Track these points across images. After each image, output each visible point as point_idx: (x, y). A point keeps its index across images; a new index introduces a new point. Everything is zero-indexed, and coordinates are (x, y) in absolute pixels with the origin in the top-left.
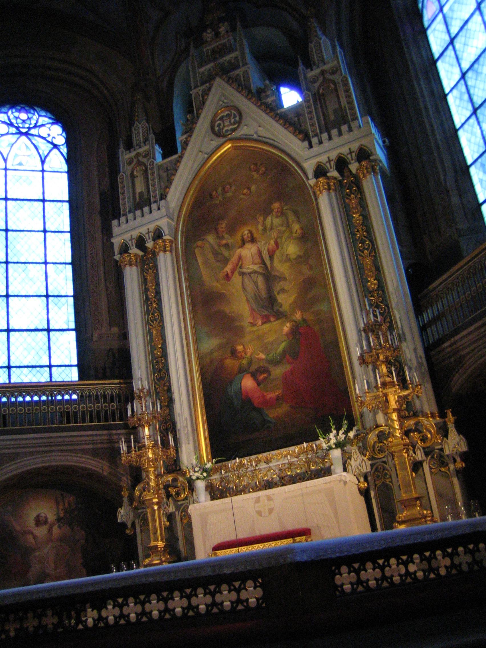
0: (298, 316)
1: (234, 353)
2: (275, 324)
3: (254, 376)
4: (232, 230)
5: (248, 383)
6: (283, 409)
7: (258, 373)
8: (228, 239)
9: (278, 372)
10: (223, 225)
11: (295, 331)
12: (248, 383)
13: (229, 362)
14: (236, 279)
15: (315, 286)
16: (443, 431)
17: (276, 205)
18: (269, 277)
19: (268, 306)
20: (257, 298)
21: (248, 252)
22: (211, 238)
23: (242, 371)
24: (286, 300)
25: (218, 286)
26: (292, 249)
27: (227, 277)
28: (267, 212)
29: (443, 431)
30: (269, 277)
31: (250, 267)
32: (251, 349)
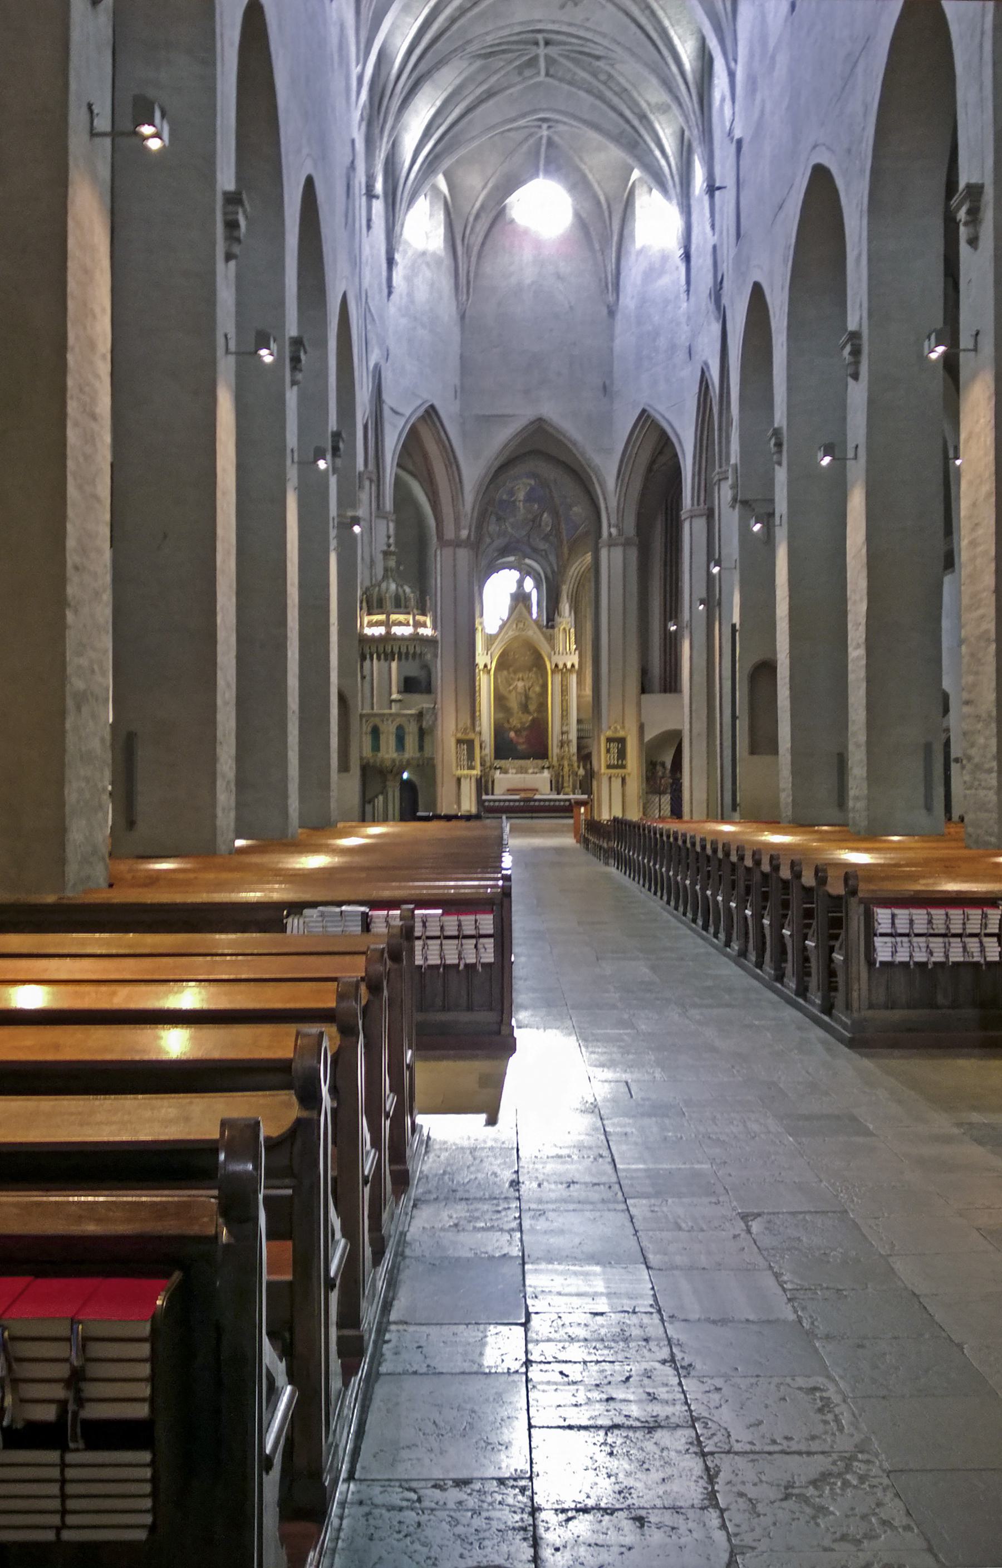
0: (535, 715)
1: (508, 722)
2: (526, 715)
3: (516, 732)
4: (515, 672)
5: (512, 734)
6: (524, 747)
7: (518, 732)
8: (512, 675)
9: (524, 733)
10: (511, 669)
11: (533, 720)
12: (512, 734)
13: (506, 725)
14: (514, 693)
15: (543, 706)
16: (579, 767)
17: (534, 669)
18: (527, 697)
19: (525, 708)
20: (521, 703)
21: (520, 684)
22: (505, 673)
23: (511, 729)
24: (532, 707)
25: (506, 693)
26: (537, 689)
27: (510, 692)
28: (530, 670)
29: (579, 767)
30: (527, 697)
31: (519, 690)
32: (515, 722)
